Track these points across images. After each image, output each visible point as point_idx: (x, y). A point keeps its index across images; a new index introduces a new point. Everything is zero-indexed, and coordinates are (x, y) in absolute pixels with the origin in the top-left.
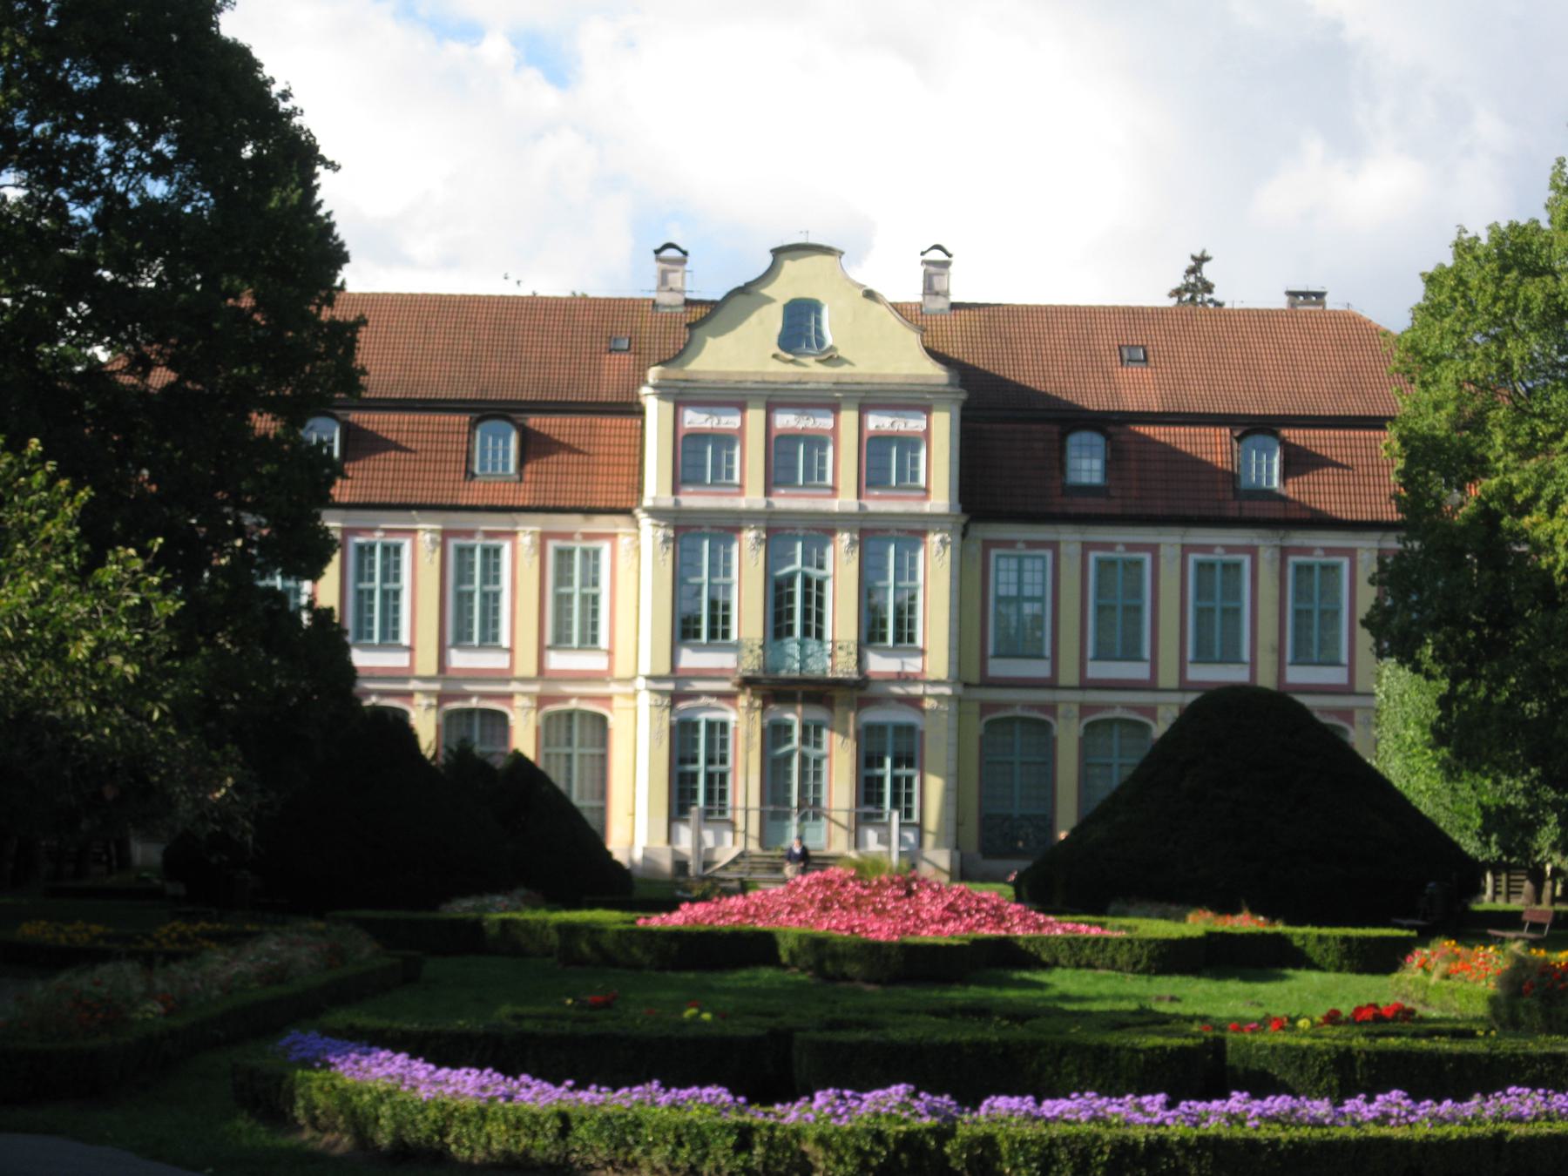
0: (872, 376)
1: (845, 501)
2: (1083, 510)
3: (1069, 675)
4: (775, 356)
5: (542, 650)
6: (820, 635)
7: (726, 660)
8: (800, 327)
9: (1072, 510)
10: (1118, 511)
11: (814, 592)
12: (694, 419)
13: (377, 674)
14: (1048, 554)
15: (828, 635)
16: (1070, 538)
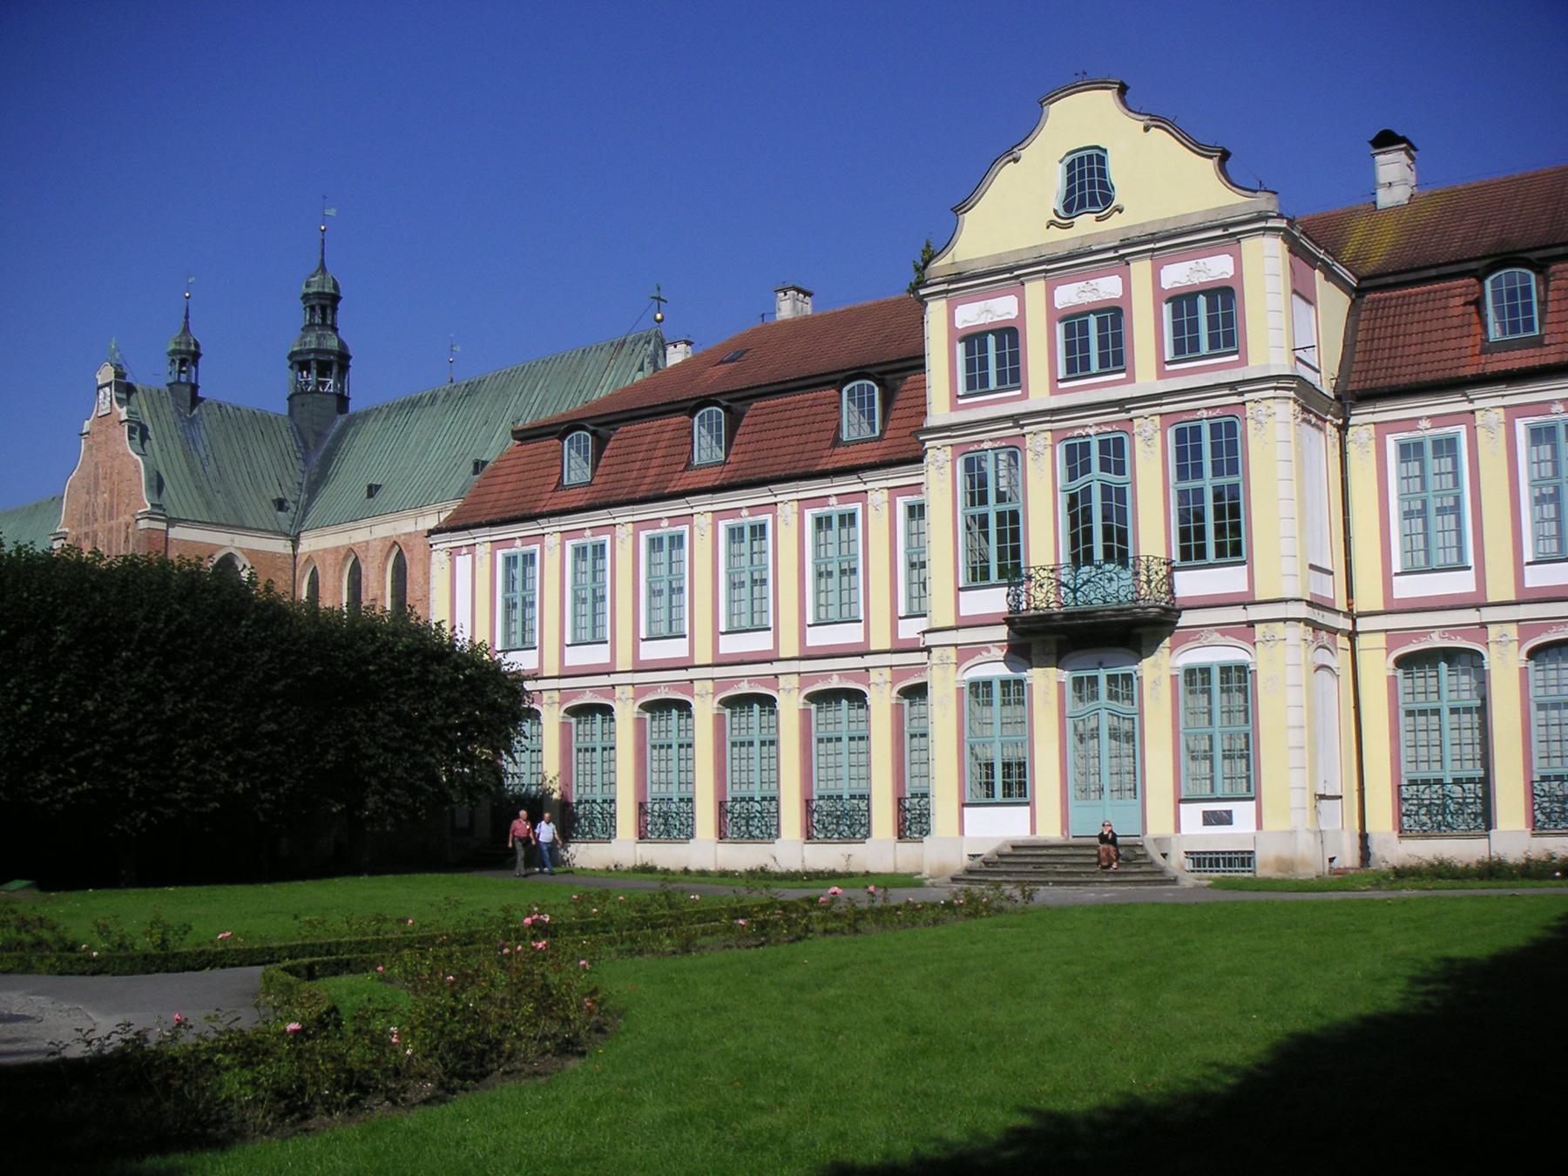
0: (1166, 220)
1: (1146, 379)
2: (1502, 367)
3: (1500, 586)
4: (1052, 223)
5: (895, 618)
6: (1123, 554)
7: (995, 600)
8: (1088, 183)
9: (1489, 369)
10: (1551, 360)
11: (1117, 500)
12: (972, 315)
13: (746, 659)
14: (1463, 429)
15: (1131, 554)
16: (1490, 405)
